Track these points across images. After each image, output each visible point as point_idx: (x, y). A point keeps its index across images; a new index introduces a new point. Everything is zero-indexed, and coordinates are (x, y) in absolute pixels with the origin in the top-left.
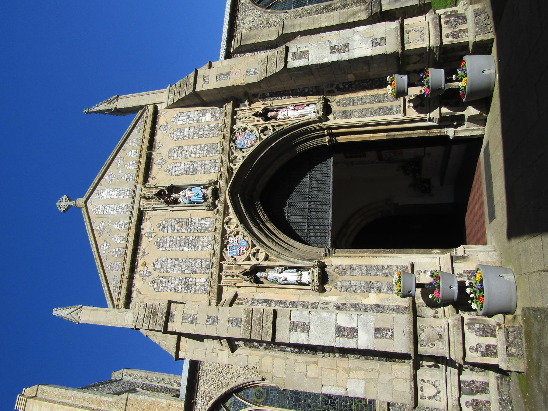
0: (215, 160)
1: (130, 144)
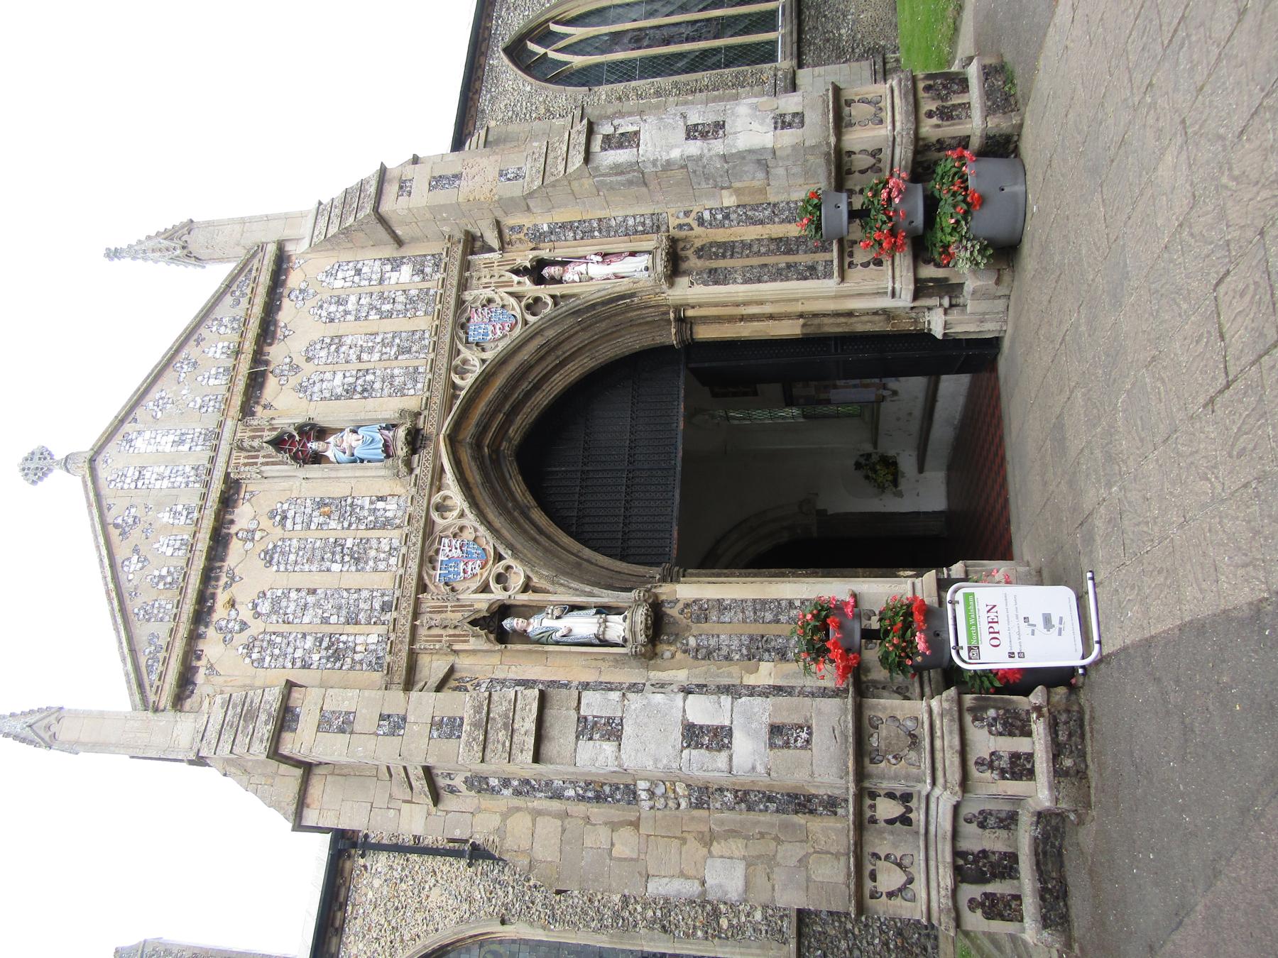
0: (416, 369)
1: (214, 329)
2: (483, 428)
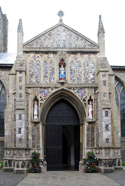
0: (75, 81)
2: (65, 94)
